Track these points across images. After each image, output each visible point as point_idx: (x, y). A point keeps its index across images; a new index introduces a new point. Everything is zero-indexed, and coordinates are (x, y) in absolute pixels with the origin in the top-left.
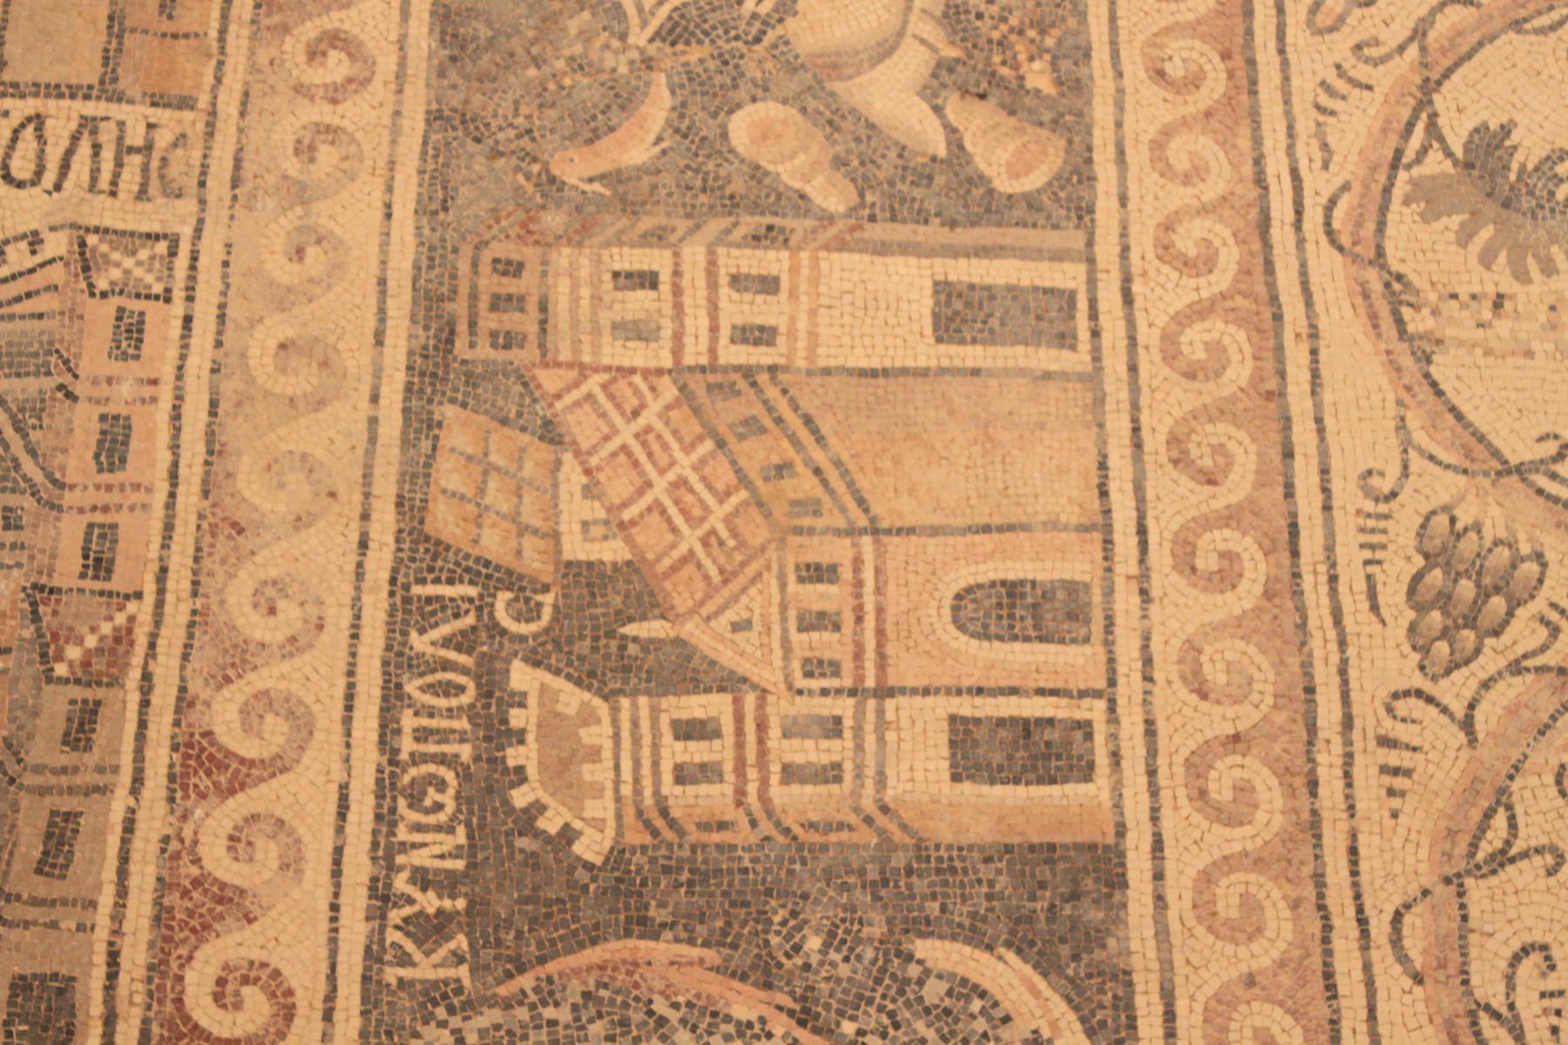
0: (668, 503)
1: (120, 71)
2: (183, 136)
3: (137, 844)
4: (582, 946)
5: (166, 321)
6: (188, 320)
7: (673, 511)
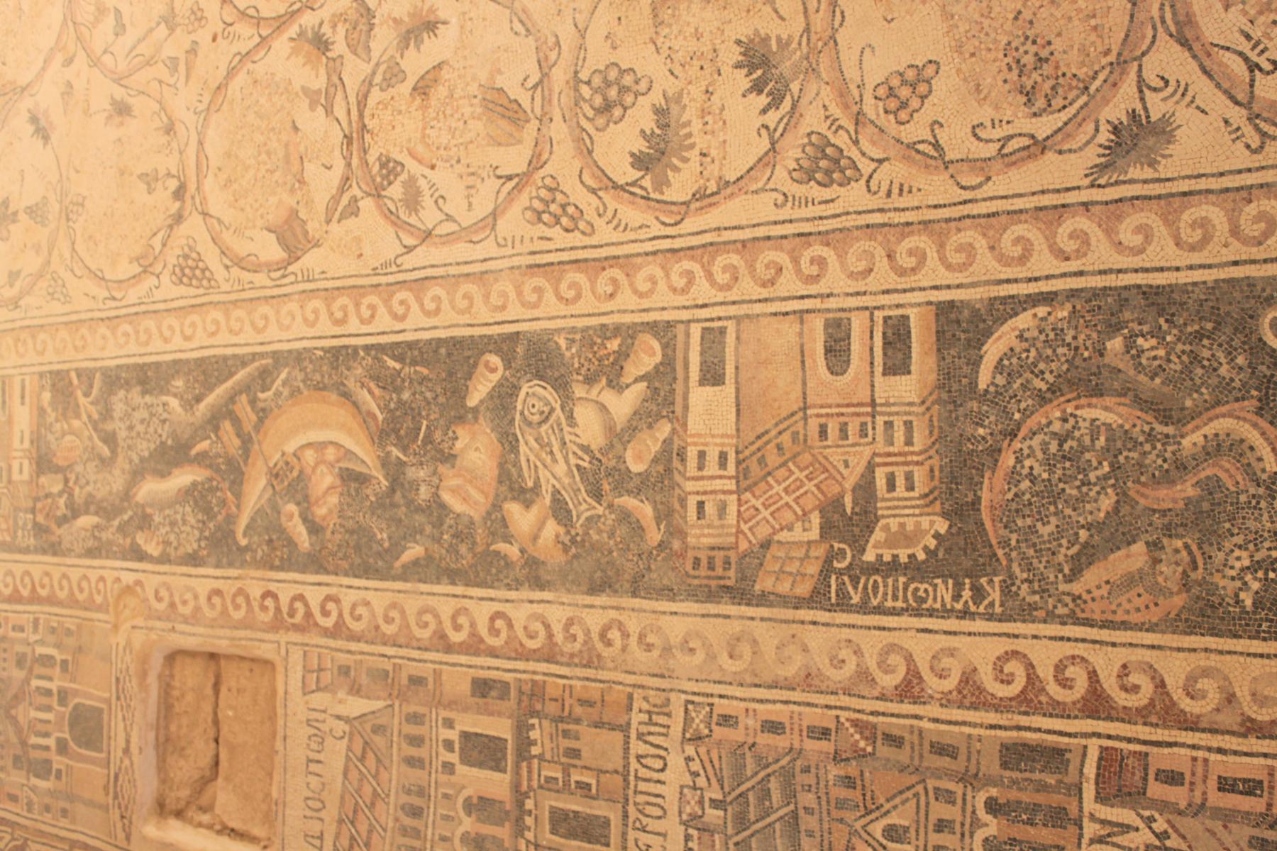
0: (794, 496)
3: (943, 717)
4: (984, 529)
5: (721, 705)
6: (721, 696)
7: (798, 494)
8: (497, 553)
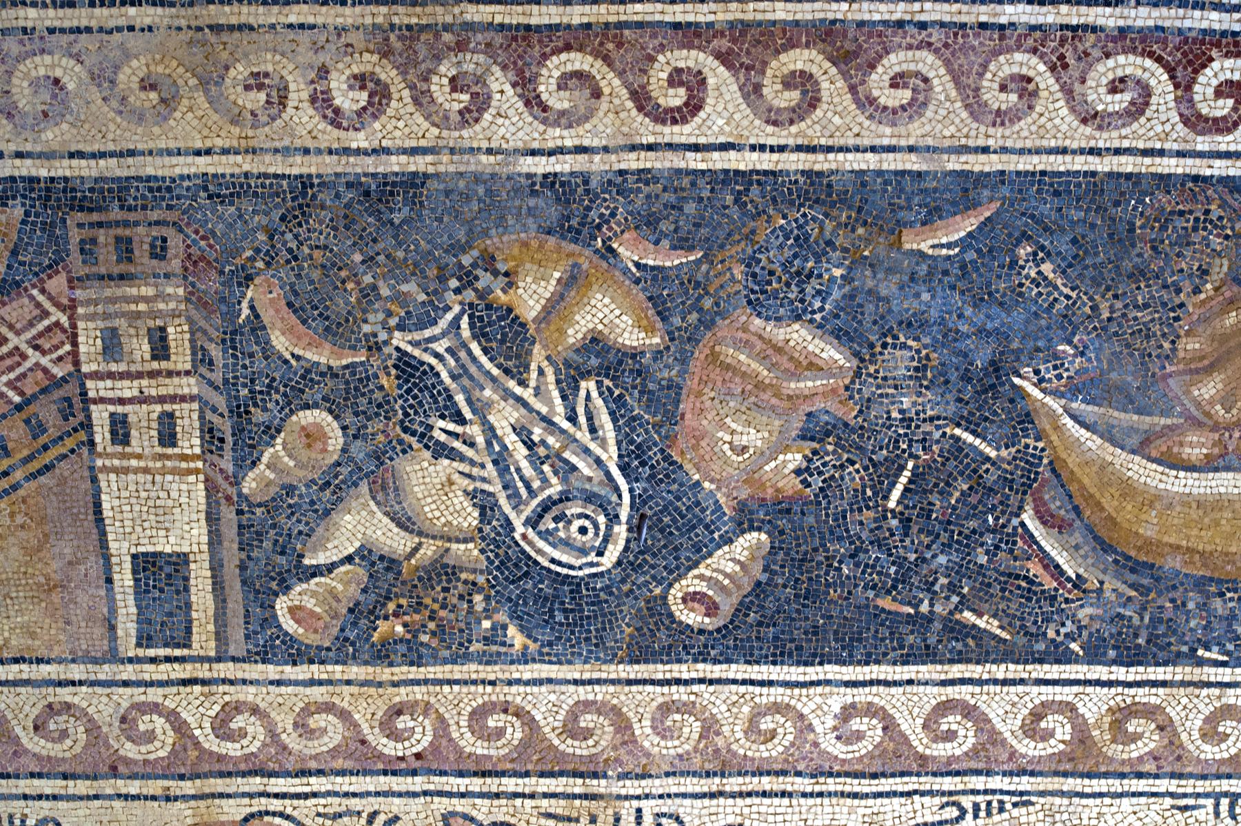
8: (682, 244)
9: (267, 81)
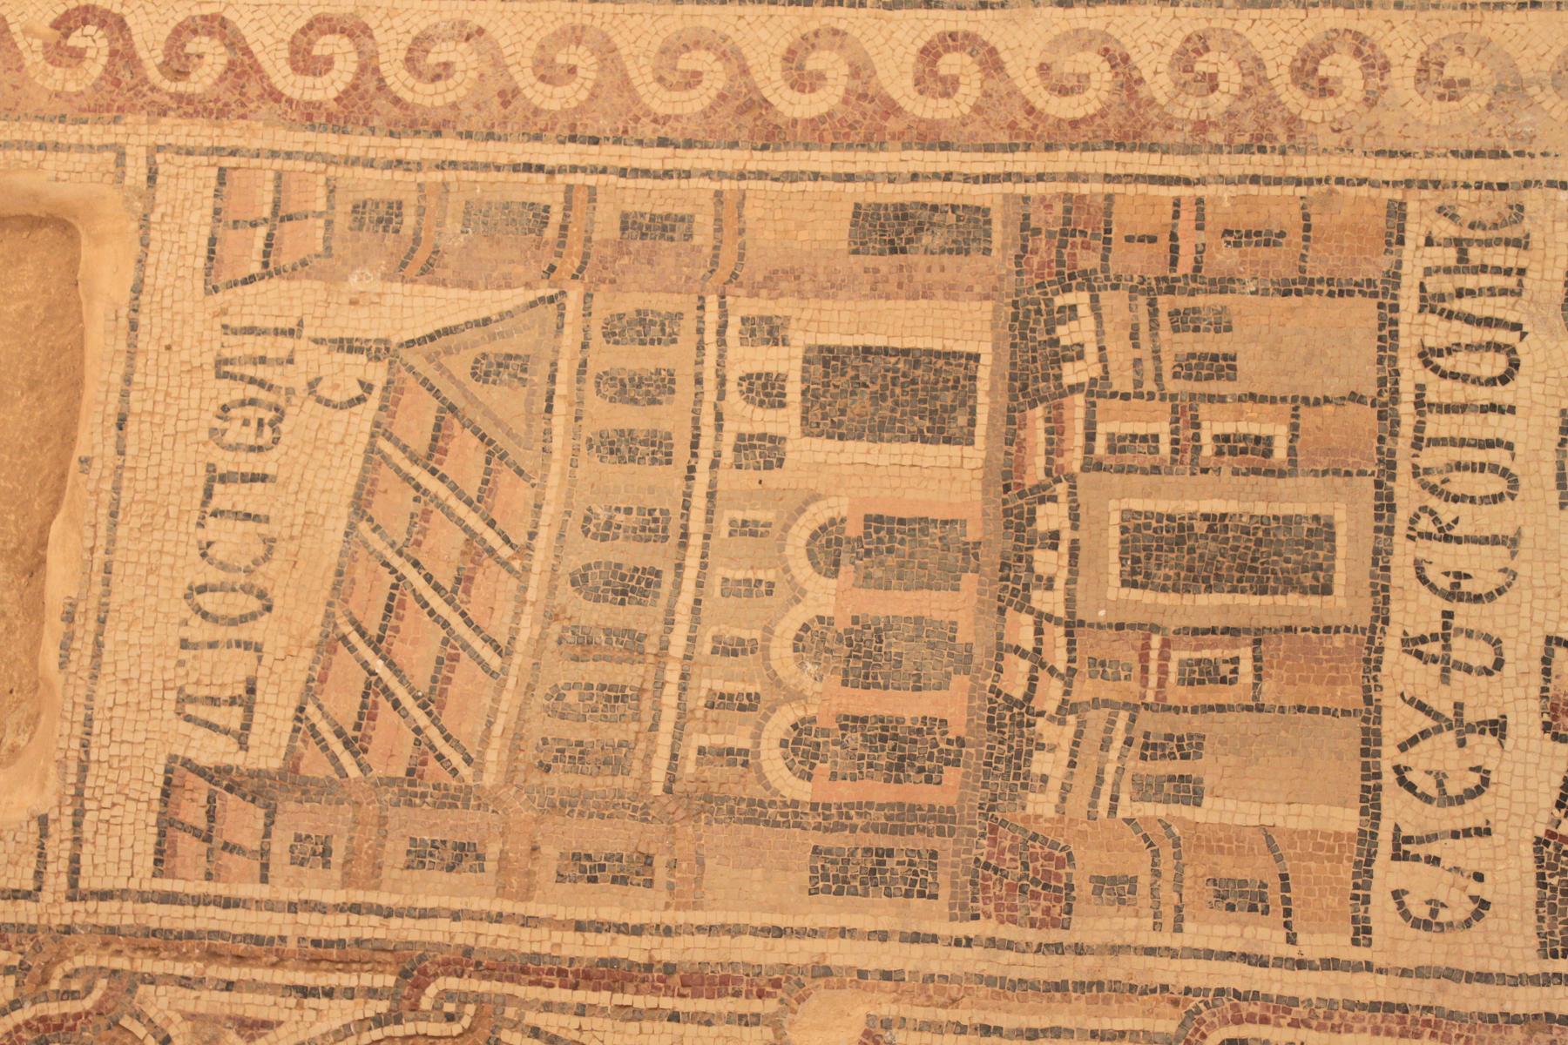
1: (1358, 278)
2: (1440, 210)
9: (1441, 90)
